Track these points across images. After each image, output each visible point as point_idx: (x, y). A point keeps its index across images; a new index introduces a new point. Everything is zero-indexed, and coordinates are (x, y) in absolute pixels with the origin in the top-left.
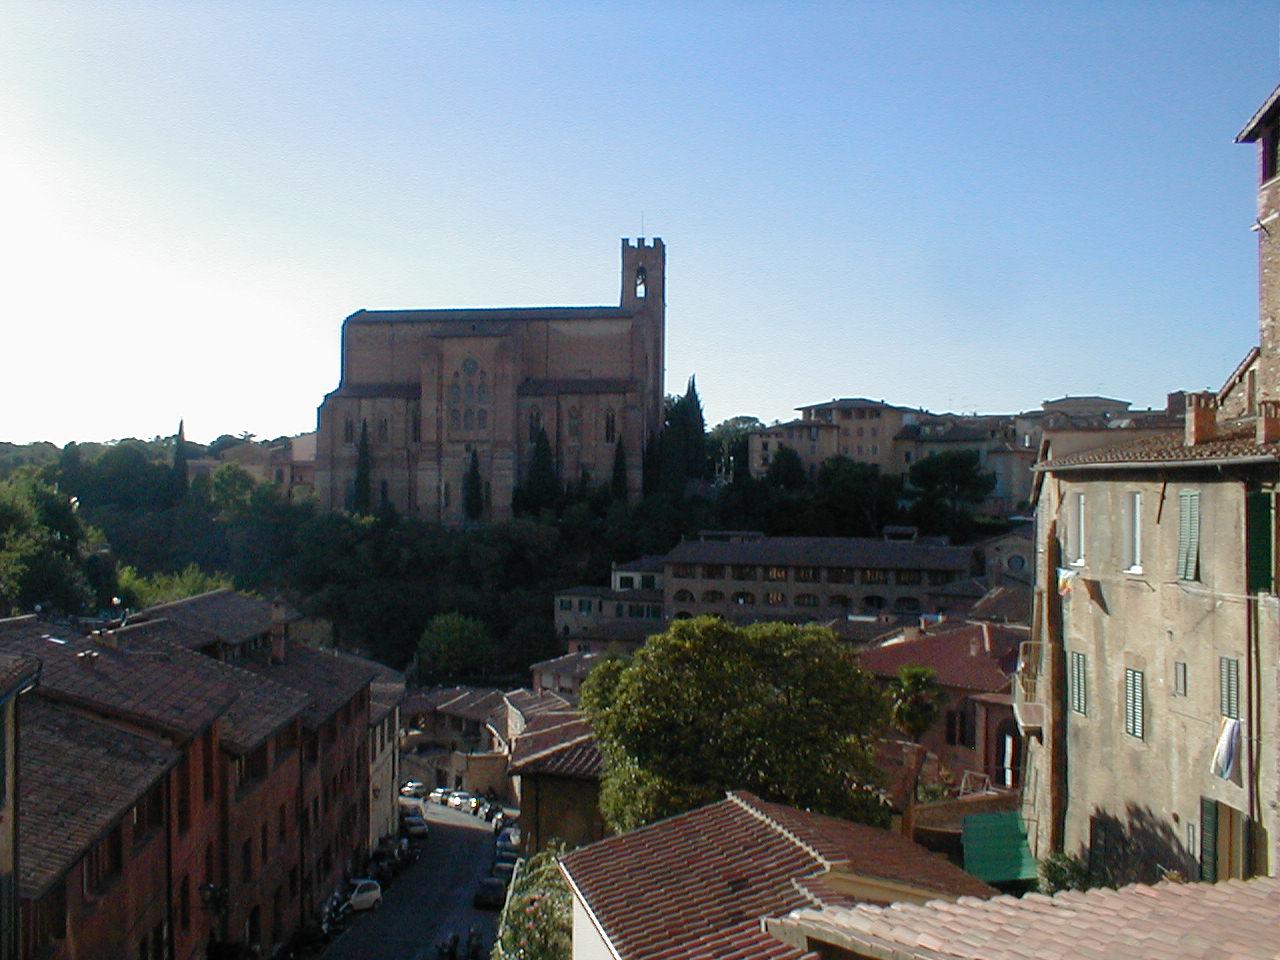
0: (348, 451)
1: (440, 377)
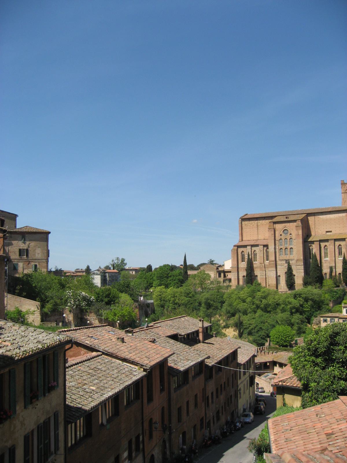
0: (243, 265)
1: (275, 237)
